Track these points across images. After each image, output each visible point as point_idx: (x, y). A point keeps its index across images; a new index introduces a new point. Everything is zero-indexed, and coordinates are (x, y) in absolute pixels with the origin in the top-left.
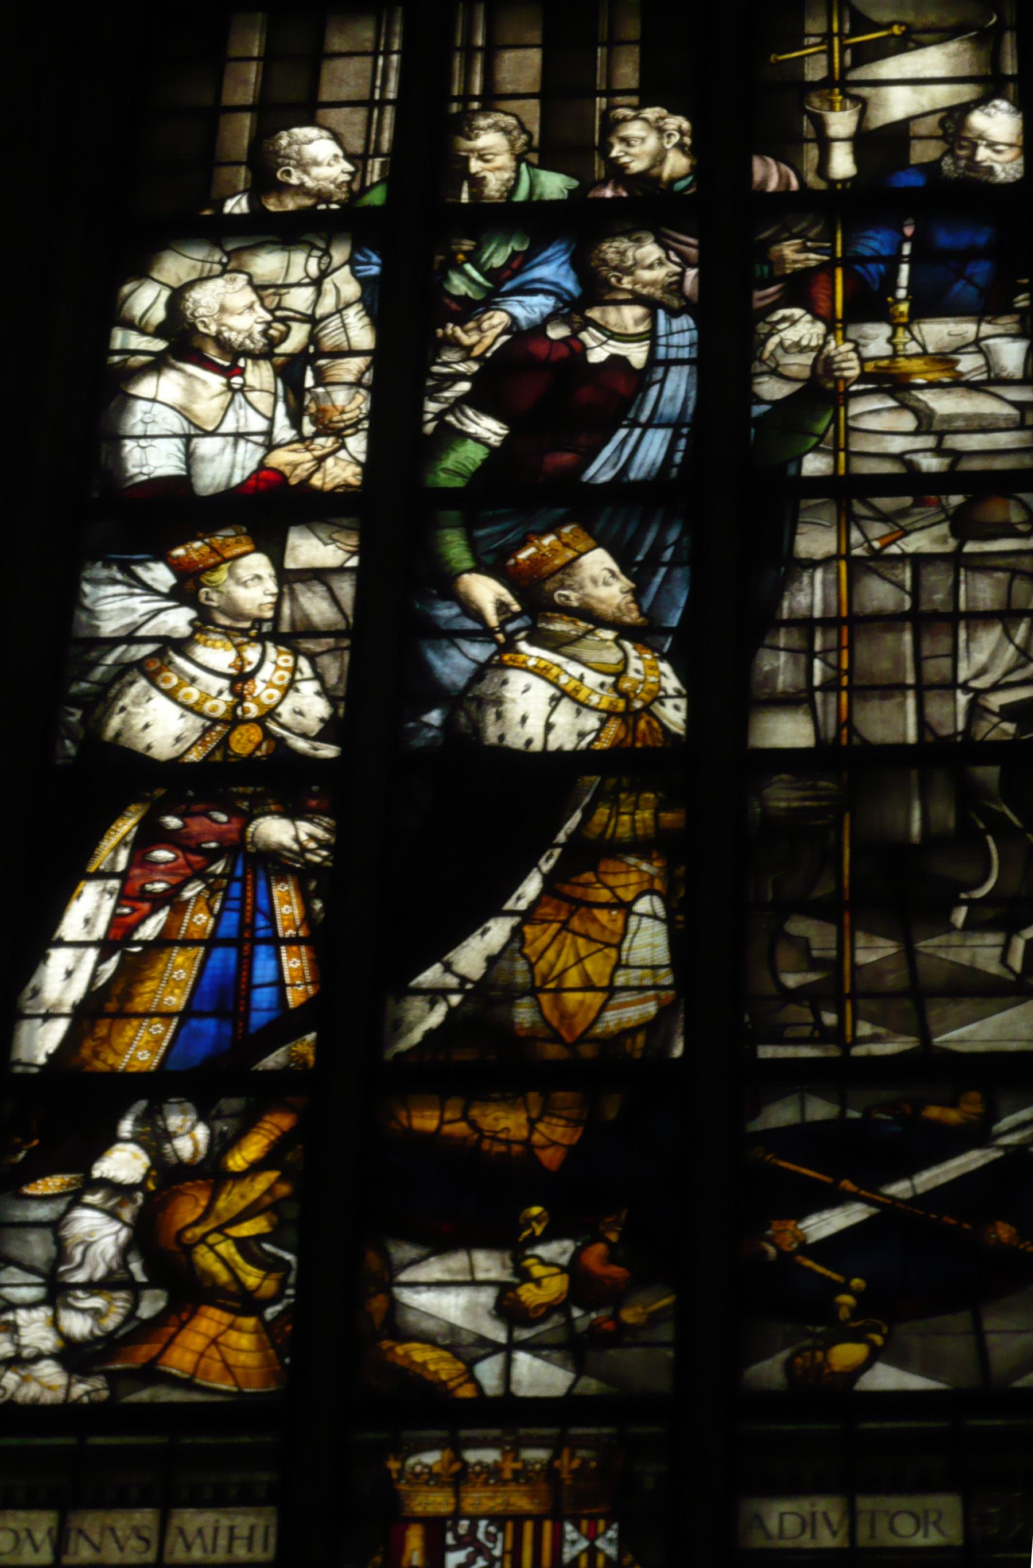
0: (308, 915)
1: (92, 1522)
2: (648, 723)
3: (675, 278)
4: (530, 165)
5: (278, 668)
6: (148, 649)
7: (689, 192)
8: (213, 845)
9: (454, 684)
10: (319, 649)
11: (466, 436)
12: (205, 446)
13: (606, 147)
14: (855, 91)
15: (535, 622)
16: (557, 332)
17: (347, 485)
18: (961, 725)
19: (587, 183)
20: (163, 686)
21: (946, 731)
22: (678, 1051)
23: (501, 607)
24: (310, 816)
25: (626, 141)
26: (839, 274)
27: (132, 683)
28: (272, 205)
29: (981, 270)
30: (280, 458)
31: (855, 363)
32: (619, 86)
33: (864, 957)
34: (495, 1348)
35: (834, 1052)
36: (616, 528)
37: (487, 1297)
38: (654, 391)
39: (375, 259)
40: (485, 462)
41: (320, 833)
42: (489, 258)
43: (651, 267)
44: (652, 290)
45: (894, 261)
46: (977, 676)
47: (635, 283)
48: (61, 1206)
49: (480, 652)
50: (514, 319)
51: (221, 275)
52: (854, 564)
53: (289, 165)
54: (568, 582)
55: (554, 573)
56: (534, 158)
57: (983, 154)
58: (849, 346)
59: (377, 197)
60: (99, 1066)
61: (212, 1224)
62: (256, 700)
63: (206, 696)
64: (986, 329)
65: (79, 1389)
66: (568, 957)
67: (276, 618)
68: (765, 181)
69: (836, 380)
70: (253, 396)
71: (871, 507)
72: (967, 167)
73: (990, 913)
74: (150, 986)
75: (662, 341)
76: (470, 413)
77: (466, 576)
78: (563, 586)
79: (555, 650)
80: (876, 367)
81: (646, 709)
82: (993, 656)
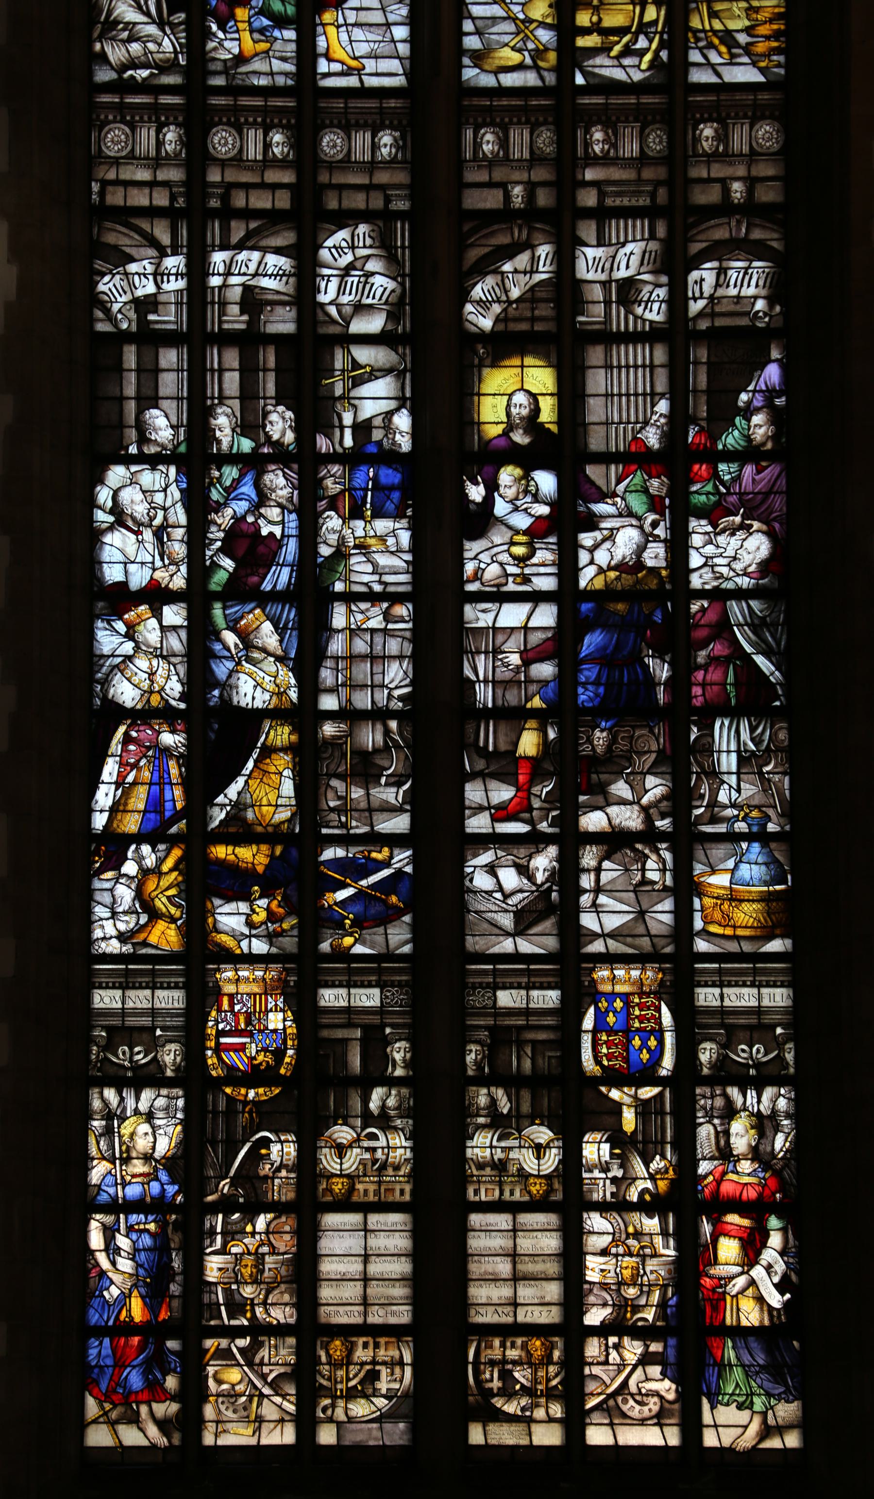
0: (181, 774)
1: (131, 993)
11: (221, 567)
12: (132, 568)
14: (353, 401)
16: (250, 519)
19: (258, 446)
21: (380, 705)
22: (297, 830)
23: (236, 645)
25: (271, 423)
29: (396, 496)
30: (158, 575)
32: (268, 395)
33: (354, 796)
34: (247, 936)
35: (344, 831)
37: (243, 918)
45: (366, 490)
48: (112, 883)
49: (230, 665)
52: (351, 630)
56: (238, 430)
59: (183, 449)
60: (119, 831)
61: (159, 891)
63: (140, 681)
64: (397, 525)
65: (124, 949)
66: (263, 793)
67: (161, 648)
68: (321, 448)
70: (146, 545)
73: (393, 780)
74: (133, 800)
81: (285, 692)
82: (396, 675)
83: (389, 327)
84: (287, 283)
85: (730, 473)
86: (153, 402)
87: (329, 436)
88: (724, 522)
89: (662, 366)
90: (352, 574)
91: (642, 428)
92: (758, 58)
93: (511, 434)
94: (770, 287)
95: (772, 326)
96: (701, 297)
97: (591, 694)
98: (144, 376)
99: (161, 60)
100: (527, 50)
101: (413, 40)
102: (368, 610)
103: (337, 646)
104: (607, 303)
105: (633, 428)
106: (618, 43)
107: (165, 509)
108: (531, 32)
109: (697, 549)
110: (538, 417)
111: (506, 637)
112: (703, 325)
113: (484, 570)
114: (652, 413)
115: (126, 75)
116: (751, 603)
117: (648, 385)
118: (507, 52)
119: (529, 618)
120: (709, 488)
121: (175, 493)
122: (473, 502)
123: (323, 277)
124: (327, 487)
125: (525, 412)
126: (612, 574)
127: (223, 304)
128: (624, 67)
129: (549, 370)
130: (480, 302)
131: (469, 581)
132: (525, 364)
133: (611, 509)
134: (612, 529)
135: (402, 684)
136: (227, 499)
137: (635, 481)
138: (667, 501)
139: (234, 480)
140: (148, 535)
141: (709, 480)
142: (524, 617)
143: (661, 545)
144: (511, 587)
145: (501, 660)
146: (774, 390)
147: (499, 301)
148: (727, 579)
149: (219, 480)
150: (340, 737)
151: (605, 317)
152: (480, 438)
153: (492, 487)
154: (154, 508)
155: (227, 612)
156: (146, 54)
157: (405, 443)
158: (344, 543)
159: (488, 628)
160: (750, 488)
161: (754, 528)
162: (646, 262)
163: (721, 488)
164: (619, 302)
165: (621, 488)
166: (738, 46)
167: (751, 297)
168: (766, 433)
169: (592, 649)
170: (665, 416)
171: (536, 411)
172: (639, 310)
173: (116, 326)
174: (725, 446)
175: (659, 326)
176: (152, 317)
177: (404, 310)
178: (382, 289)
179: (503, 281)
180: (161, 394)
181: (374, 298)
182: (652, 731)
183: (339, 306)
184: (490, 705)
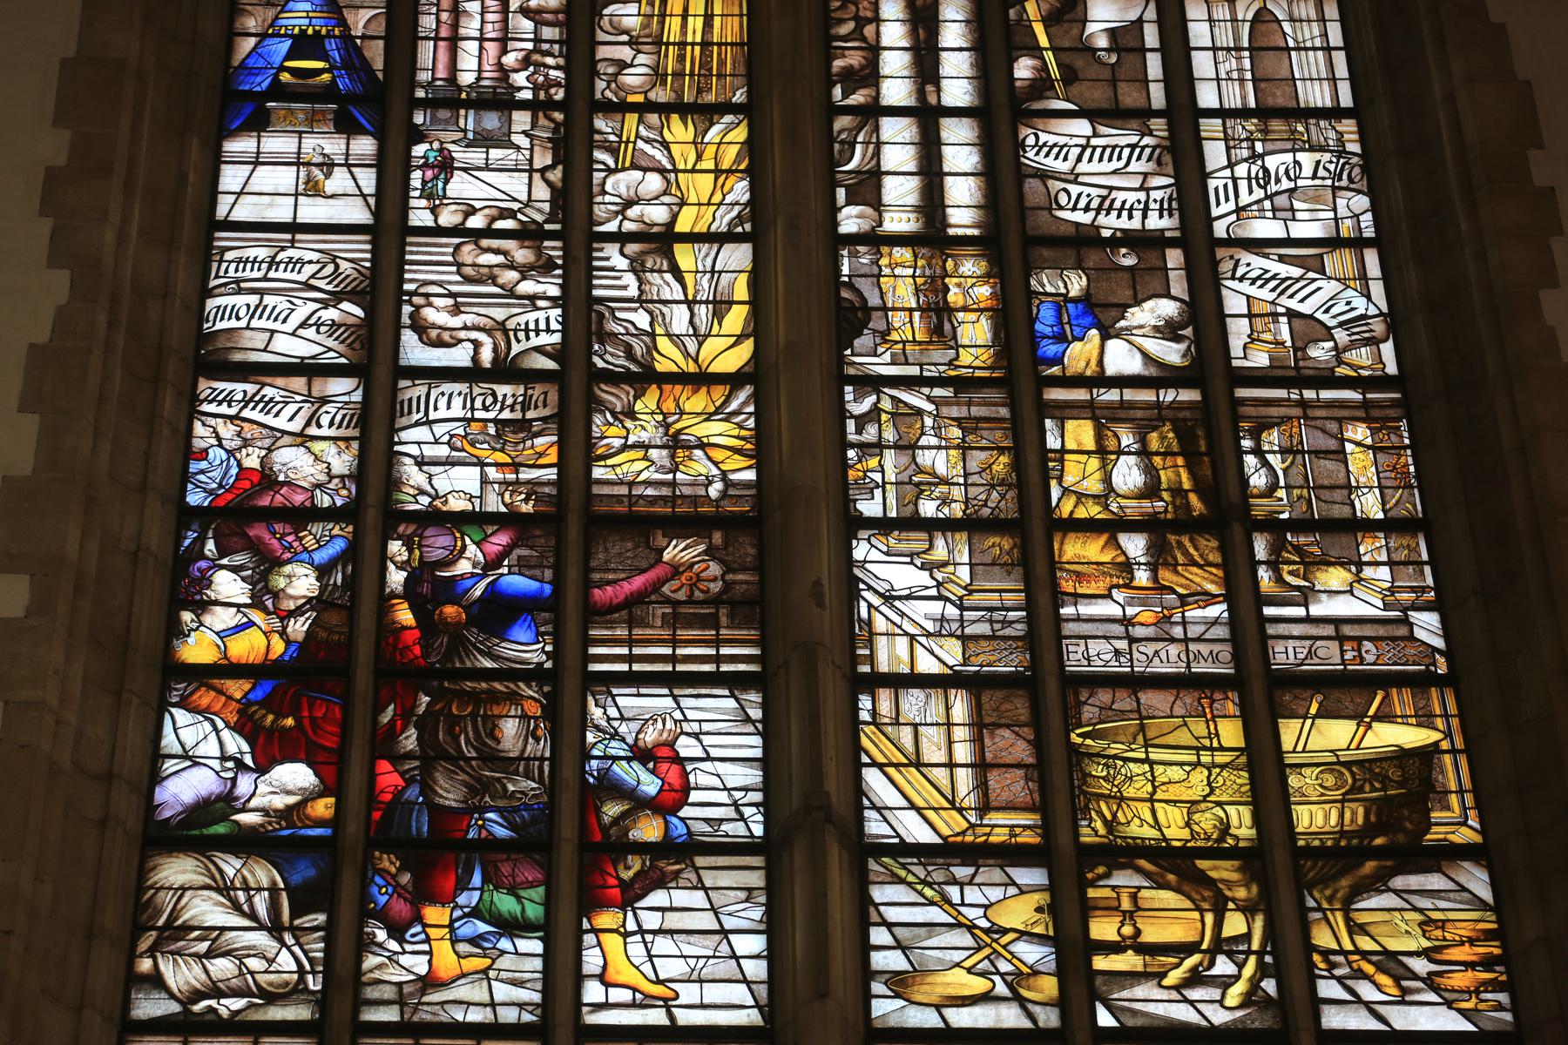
92: (1454, 996)
99: (271, 984)
100: (998, 972)
101: (772, 956)
106: (1178, 966)
108: (1004, 947)
115: (199, 1007)
118: (959, 975)
128: (1192, 1003)
156: (241, 974)
166: (1416, 977)
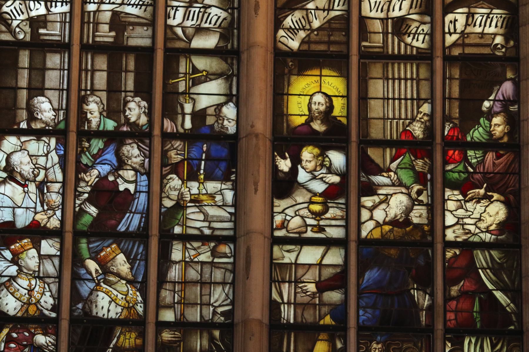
2: (134, 311)
3: (142, 162)
4: (104, 116)
5: (40, 287)
6: (6, 279)
7: (147, 130)
8: (25, 343)
9: (85, 295)
10: (50, 282)
12: (19, 211)
13: (125, 111)
14: (192, 96)
15: (105, 277)
16: (111, 178)
17: (57, 228)
18: (211, 318)
19: (119, 125)
20: (10, 291)
21: (207, 319)
23: (97, 271)
24: (49, 335)
25: (129, 109)
26: (186, 162)
27: (2, 290)
28: (33, 126)
29: (223, 165)
30: (38, 217)
31: (189, 196)
32: (128, 89)
36: (126, 247)
38: (136, 201)
39: (62, 149)
40: (92, 222)
41: (52, 341)
42: (93, 150)
43: (136, 157)
44: (136, 165)
46: (215, 302)
47: (132, 162)
49: (92, 285)
50: (99, 172)
51: (20, 151)
52: (186, 262)
53: (37, 111)
54: (114, 264)
55: (110, 261)
56: (105, 114)
57: (226, 123)
58: (188, 189)
59: (62, 126)
62: (35, 297)
63: (21, 295)
64: (224, 186)
67: (39, 271)
68: (167, 128)
69: (184, 201)
71: (191, 245)
72: (221, 127)
75: (139, 184)
76: (88, 204)
77: (87, 260)
78: (112, 266)
79: (110, 286)
80: (195, 197)
81: (133, 306)
82: (220, 296)
83: (221, 44)
84: (145, 11)
85: (476, 158)
86: (40, 92)
87: (173, 120)
88: (472, 193)
89: (425, 79)
90: (188, 221)
91: (410, 123)
93: (312, 124)
94: (506, 28)
95: (507, 55)
96: (455, 32)
97: (370, 316)
98: (34, 73)
102: (199, 248)
103: (174, 273)
104: (385, 33)
105: (403, 122)
107: (46, 169)
109: (451, 212)
110: (332, 112)
111: (305, 271)
112: (456, 52)
113: (289, 221)
114: (418, 112)
116: (492, 252)
117: (415, 92)
119: (323, 257)
120: (461, 168)
121: (54, 157)
122: (282, 171)
123: (172, 7)
124: (171, 157)
125: (322, 108)
126: (387, 228)
127: (97, 24)
129: (340, 79)
130: (289, 29)
131: (278, 229)
132: (323, 74)
133: (386, 181)
134: (387, 195)
135: (225, 303)
136: (94, 163)
137: (405, 161)
138: (429, 176)
139: (100, 149)
140: (32, 187)
141: (461, 162)
142: (319, 257)
143: (424, 207)
144: (310, 234)
145: (301, 288)
146: (509, 100)
147: (304, 29)
148: (473, 234)
149: (88, 149)
150: (175, 342)
151: (383, 43)
152: (288, 125)
153: (296, 161)
154: (38, 168)
155: (91, 246)
157: (231, 128)
158: (182, 198)
159: (292, 264)
160: (491, 169)
161: (495, 198)
162: (414, 6)
163: (469, 168)
164: (393, 34)
165: (394, 165)
167: (492, 34)
168: (503, 130)
169: (371, 282)
170: (428, 115)
171: (330, 108)
172: (409, 40)
173: (15, 37)
174: (472, 138)
175: (423, 51)
176: (42, 31)
177: (233, 33)
178: (216, 17)
179: (307, 15)
180: (47, 86)
181: (210, 23)
182: (415, 345)
183: (184, 29)
184: (292, 321)
